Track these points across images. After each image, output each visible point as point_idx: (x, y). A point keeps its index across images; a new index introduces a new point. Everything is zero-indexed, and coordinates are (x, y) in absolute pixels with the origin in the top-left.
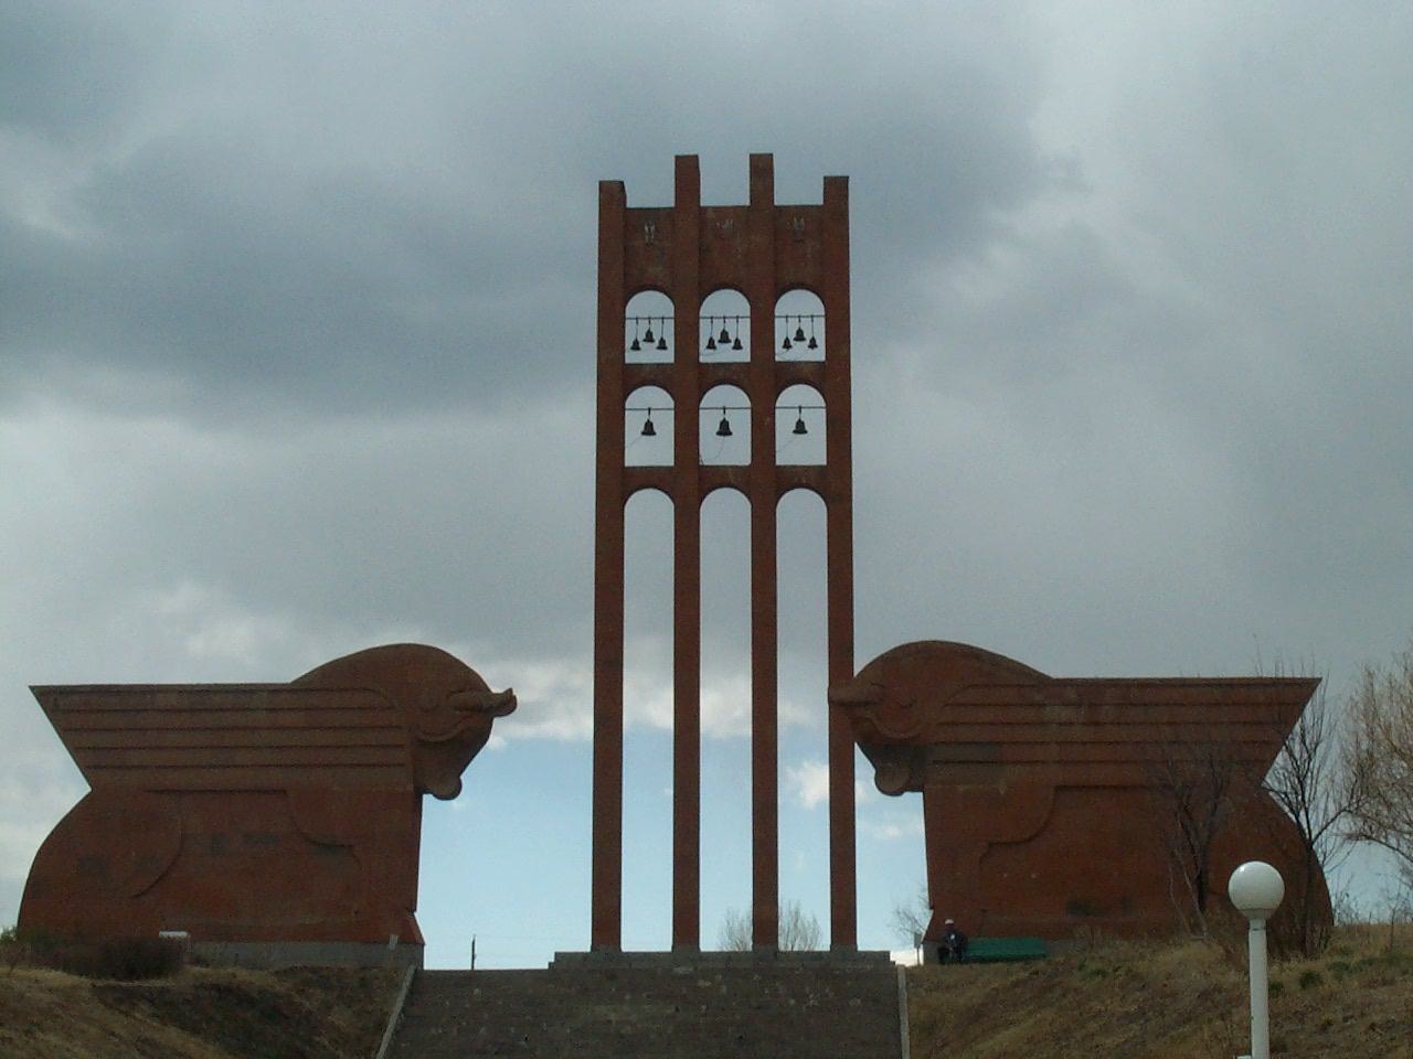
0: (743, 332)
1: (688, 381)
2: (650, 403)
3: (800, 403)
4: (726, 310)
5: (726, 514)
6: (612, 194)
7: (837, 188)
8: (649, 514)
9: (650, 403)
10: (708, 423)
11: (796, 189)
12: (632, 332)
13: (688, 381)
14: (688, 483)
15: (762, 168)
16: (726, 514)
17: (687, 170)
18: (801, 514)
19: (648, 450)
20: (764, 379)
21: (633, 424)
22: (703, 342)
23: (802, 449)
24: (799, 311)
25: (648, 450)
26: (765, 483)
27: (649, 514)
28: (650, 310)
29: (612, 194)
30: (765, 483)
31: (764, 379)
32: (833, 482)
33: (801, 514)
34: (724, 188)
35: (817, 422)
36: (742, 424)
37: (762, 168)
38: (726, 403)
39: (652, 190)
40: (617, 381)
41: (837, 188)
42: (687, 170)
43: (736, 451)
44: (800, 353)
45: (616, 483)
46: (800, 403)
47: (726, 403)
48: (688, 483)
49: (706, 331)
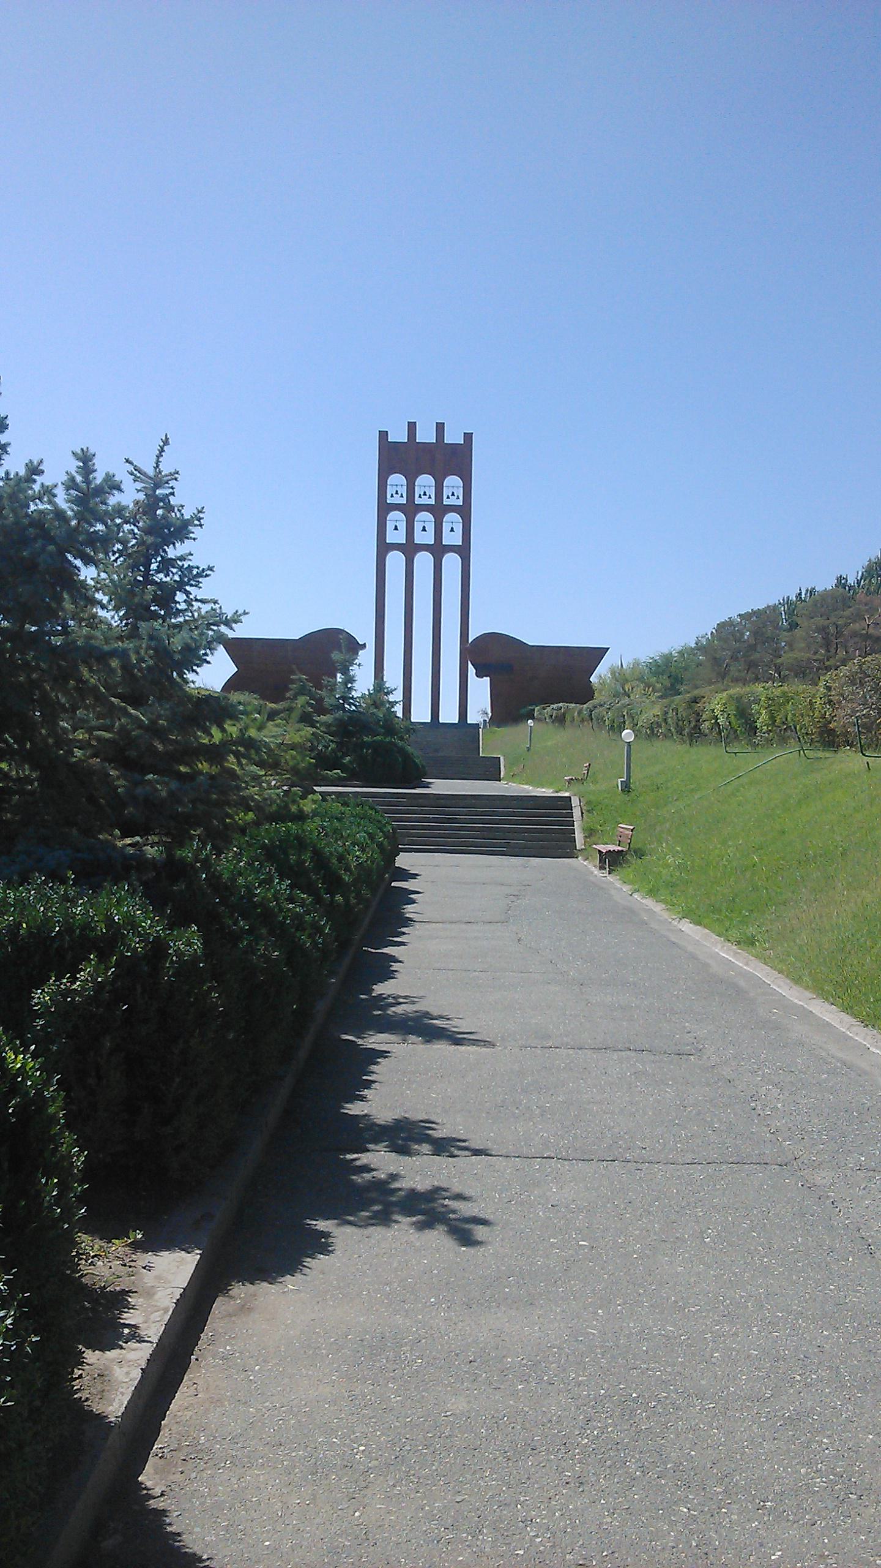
0: (432, 492)
1: (411, 510)
2: (396, 518)
3: (452, 520)
4: (425, 481)
5: (424, 562)
6: (383, 435)
7: (468, 437)
8: (395, 561)
9: (396, 518)
10: (418, 527)
11: (453, 437)
12: (390, 491)
13: (411, 510)
14: (410, 549)
15: (440, 427)
16: (424, 562)
17: (412, 426)
18: (452, 563)
19: (395, 536)
20: (439, 510)
21: (390, 526)
22: (417, 496)
23: (452, 538)
24: (453, 483)
25: (395, 536)
26: (438, 550)
27: (395, 561)
28: (397, 481)
29: (383, 435)
30: (438, 550)
31: (439, 510)
32: (464, 551)
33: (452, 563)
34: (426, 435)
35: (459, 528)
36: (430, 528)
37: (440, 427)
38: (425, 518)
39: (399, 435)
40: (384, 508)
41: (468, 437)
42: (412, 426)
43: (428, 538)
44: (453, 501)
45: (384, 548)
46: (452, 520)
47: (425, 518)
48: (410, 549)
49: (418, 491)
